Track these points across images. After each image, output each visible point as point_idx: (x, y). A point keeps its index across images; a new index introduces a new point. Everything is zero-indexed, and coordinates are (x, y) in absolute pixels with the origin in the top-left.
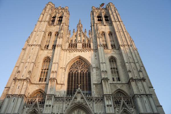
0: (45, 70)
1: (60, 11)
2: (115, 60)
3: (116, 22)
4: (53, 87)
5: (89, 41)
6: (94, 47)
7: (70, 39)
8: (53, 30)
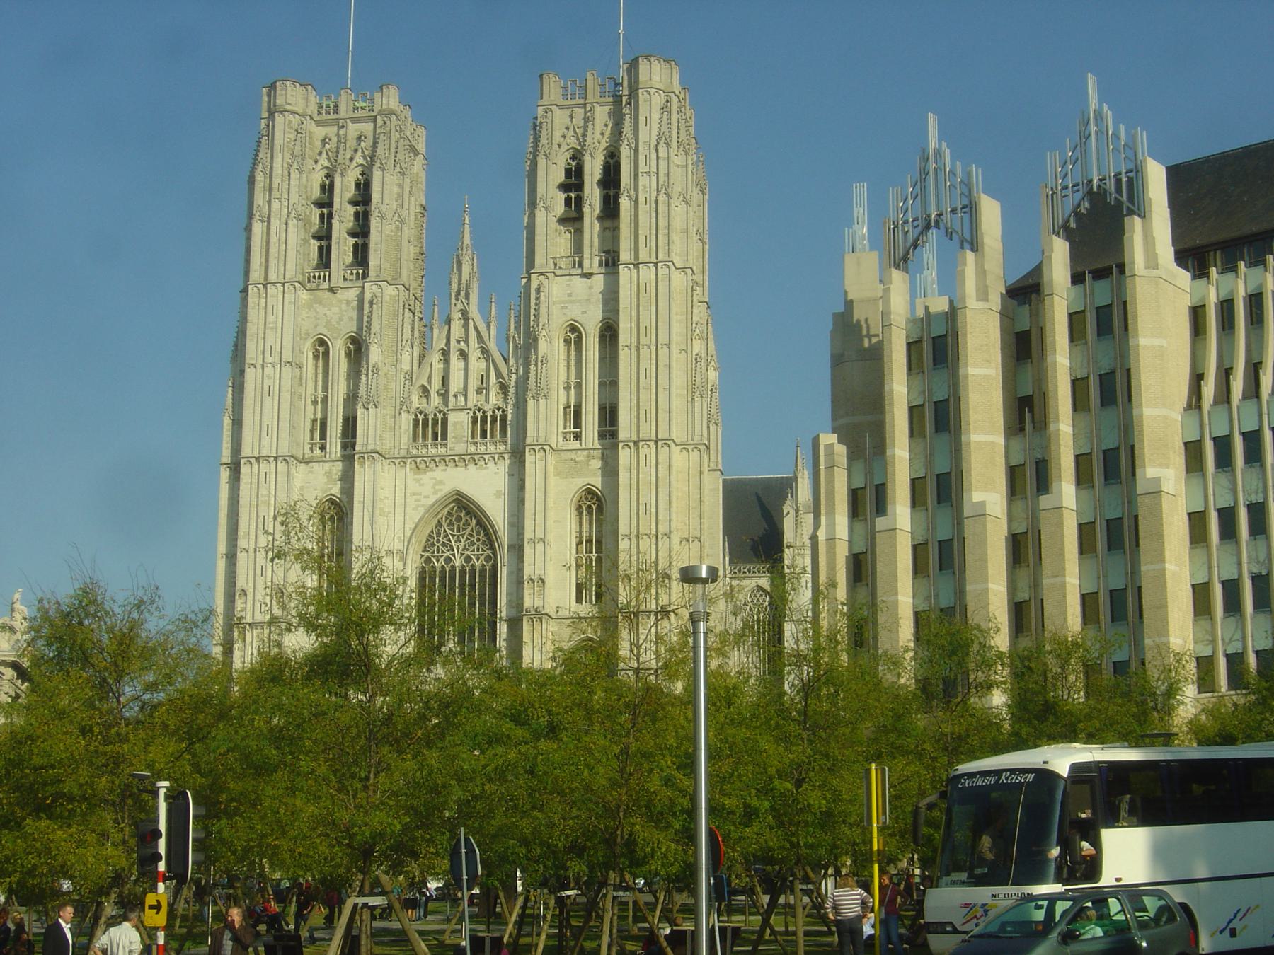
3: (636, 266)
5: (504, 388)
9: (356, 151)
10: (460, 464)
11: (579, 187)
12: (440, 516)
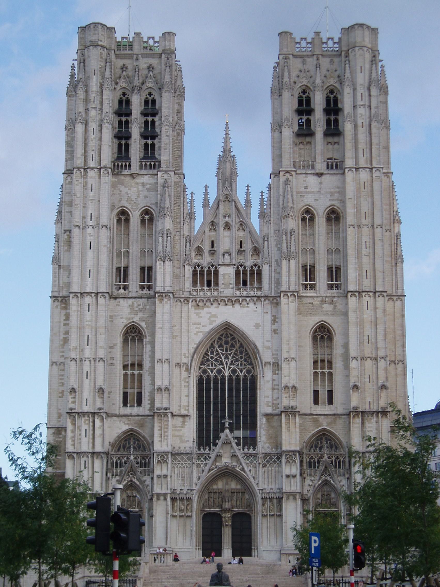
0: (133, 365)
1: (144, 63)
2: (329, 336)
3: (357, 169)
4: (166, 430)
6: (270, 284)
7: (196, 246)
9: (147, 77)
10: (229, 304)
11: (310, 112)
12: (213, 340)
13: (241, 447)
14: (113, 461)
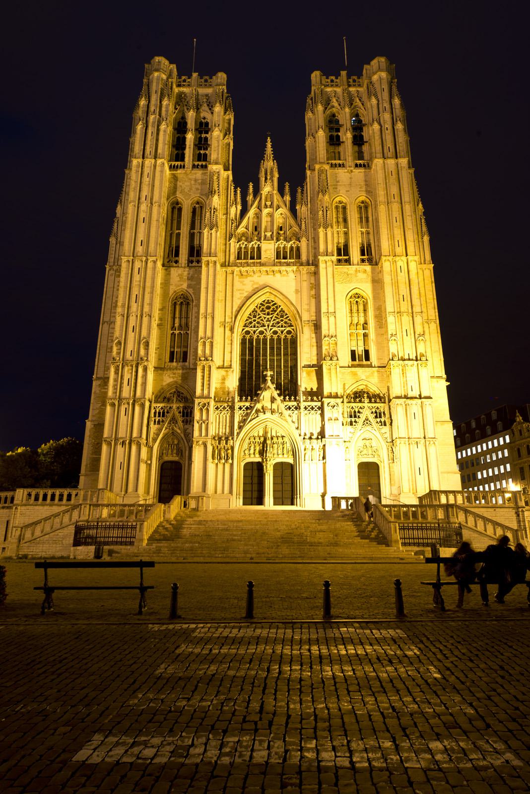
8: (186, 190)
13: (282, 397)
14: (156, 411)
